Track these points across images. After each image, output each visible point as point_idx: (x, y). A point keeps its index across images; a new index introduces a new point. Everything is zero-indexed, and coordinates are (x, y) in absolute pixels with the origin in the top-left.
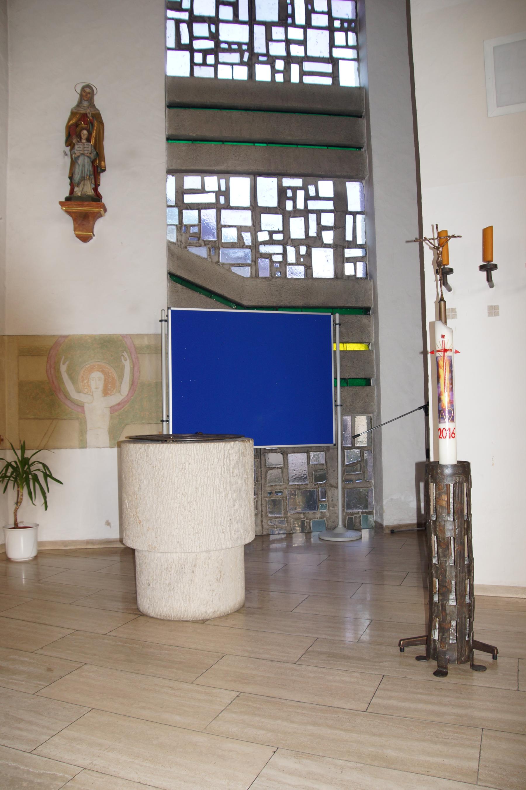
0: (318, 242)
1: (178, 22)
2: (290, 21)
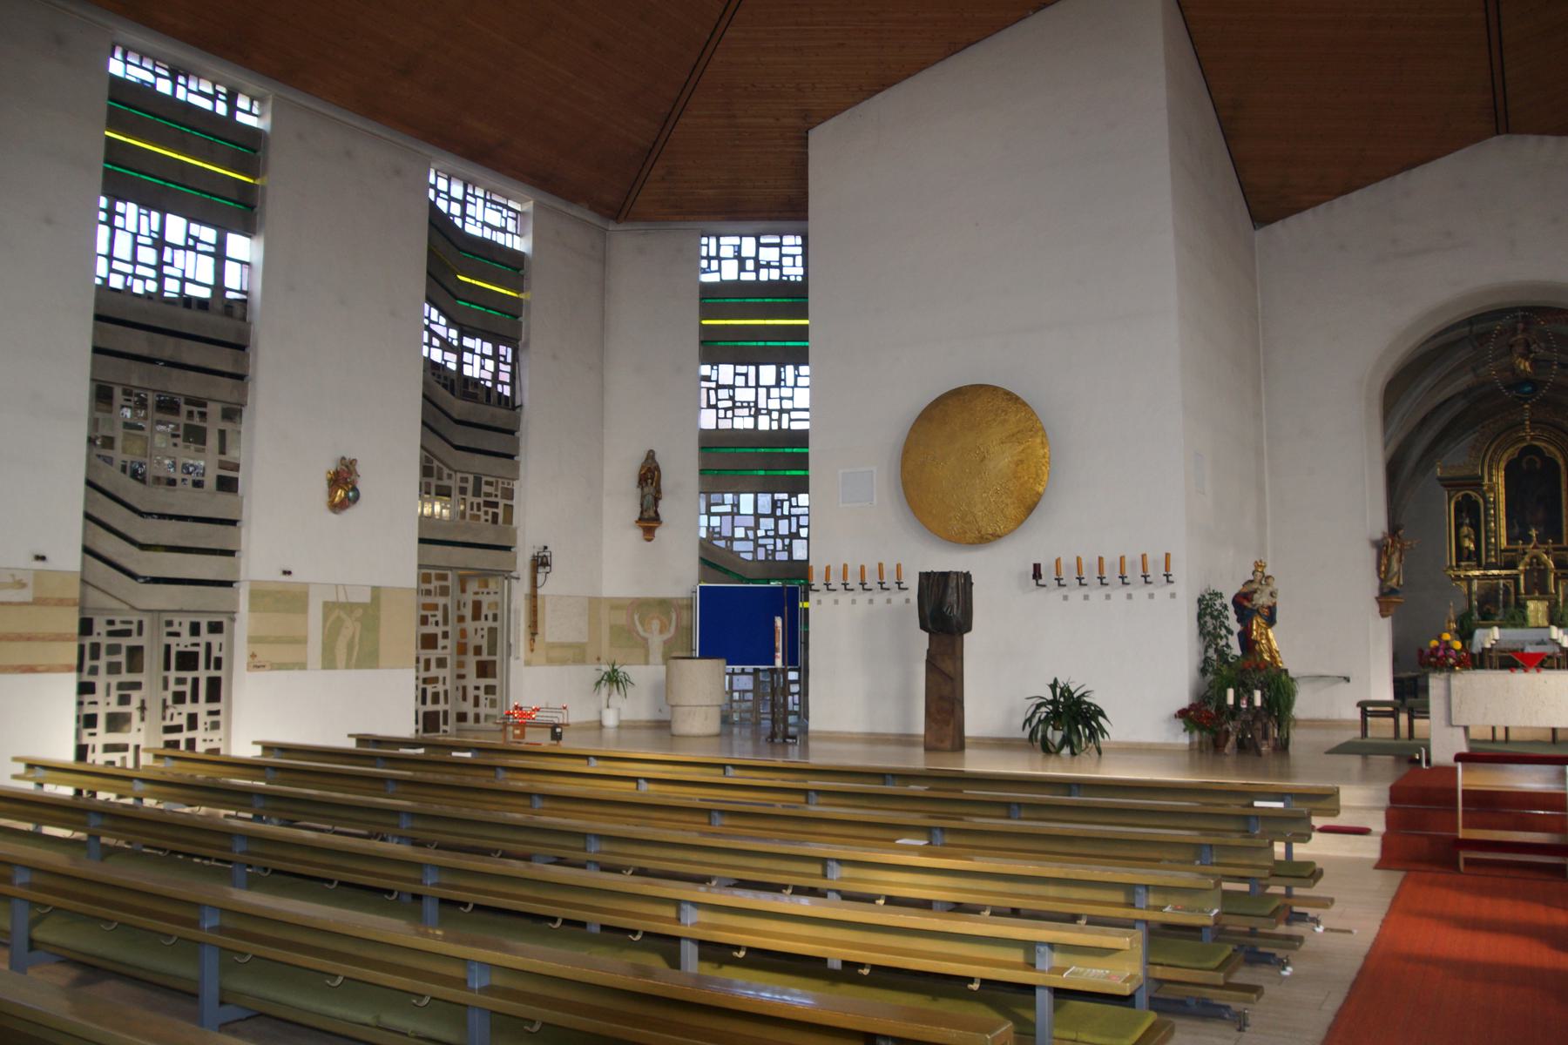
0: (797, 536)
1: (709, 389)
2: (783, 383)
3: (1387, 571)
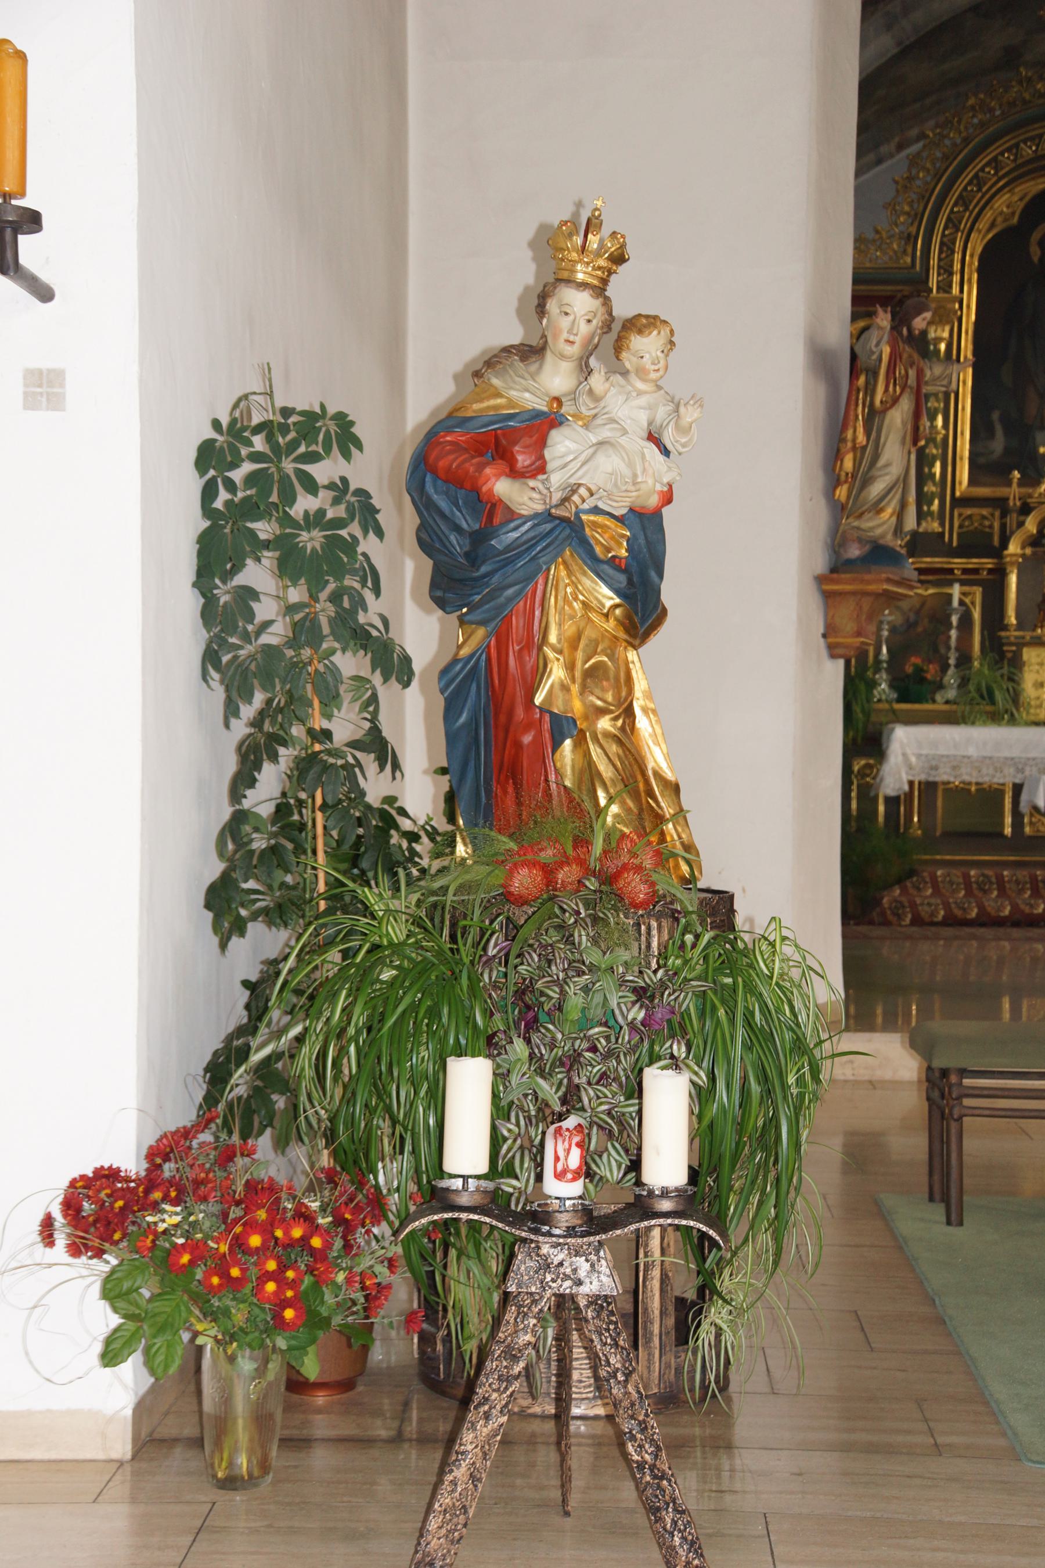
3: (863, 479)
